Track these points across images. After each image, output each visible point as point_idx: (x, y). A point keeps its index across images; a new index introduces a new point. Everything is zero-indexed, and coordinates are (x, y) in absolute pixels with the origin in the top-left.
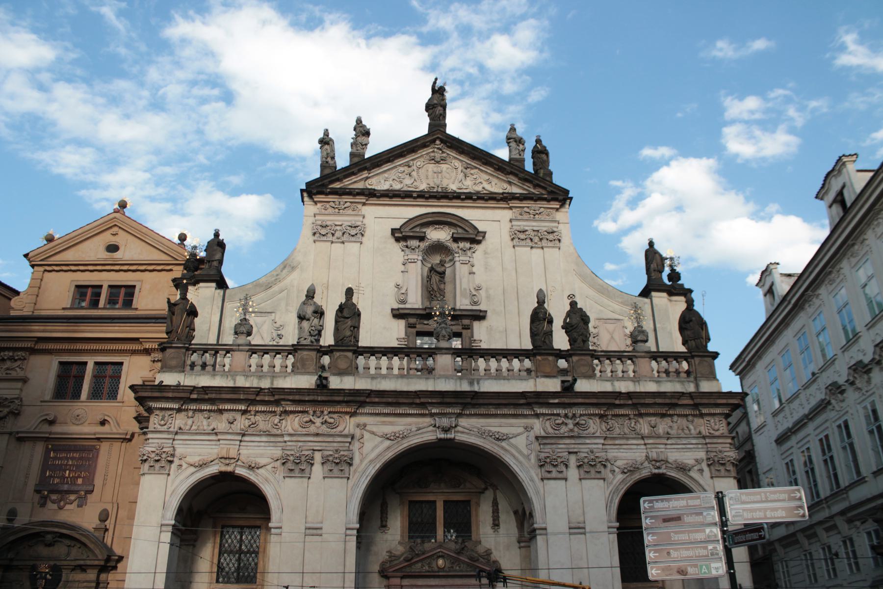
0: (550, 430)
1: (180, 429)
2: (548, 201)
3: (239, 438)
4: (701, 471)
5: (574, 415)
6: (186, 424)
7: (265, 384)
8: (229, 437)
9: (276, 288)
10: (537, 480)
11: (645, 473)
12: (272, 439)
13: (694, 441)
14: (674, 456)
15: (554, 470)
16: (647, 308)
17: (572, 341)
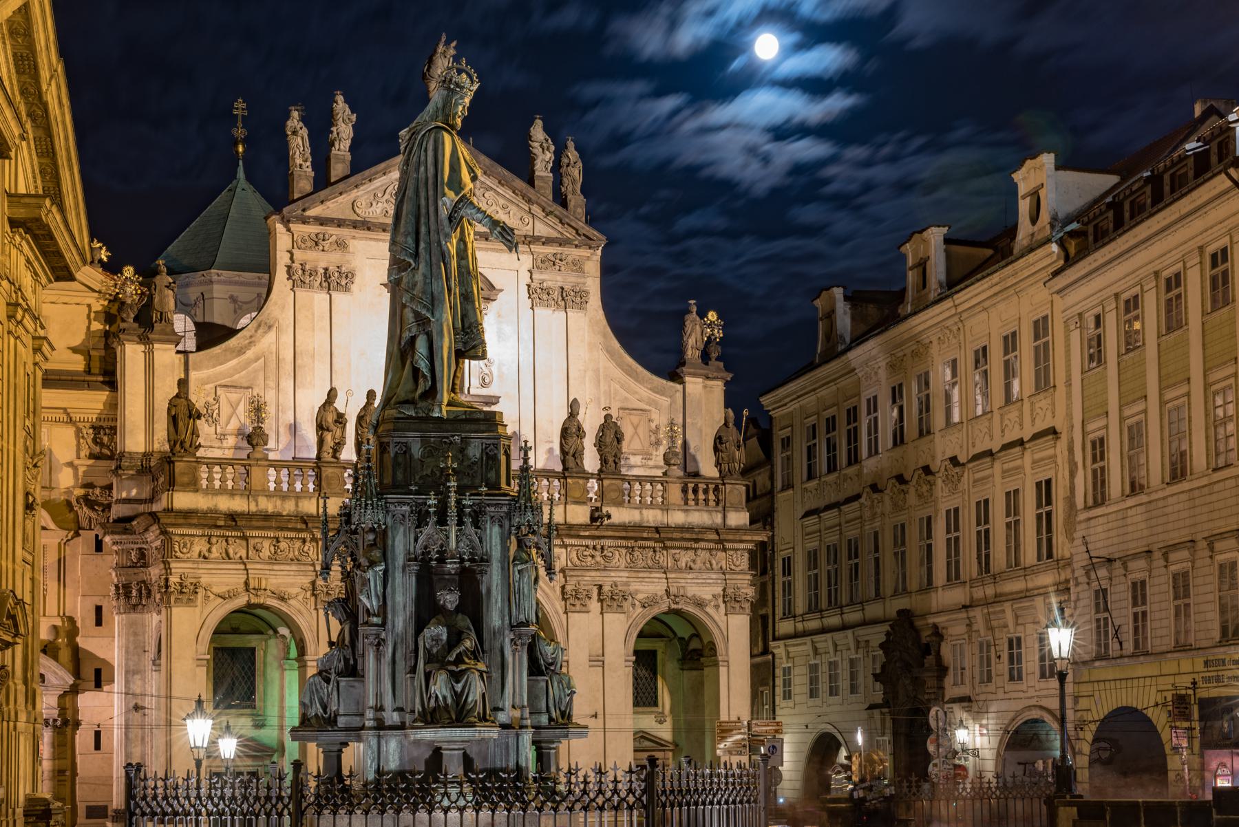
0: (578, 563)
1: (205, 557)
2: (576, 246)
3: (270, 567)
4: (717, 607)
5: (602, 548)
6: (209, 551)
7: (289, 507)
8: (259, 566)
9: (250, 354)
10: (561, 611)
11: (664, 607)
12: (303, 568)
13: (714, 576)
14: (692, 590)
15: (578, 603)
16: (679, 396)
17: (604, 461)
